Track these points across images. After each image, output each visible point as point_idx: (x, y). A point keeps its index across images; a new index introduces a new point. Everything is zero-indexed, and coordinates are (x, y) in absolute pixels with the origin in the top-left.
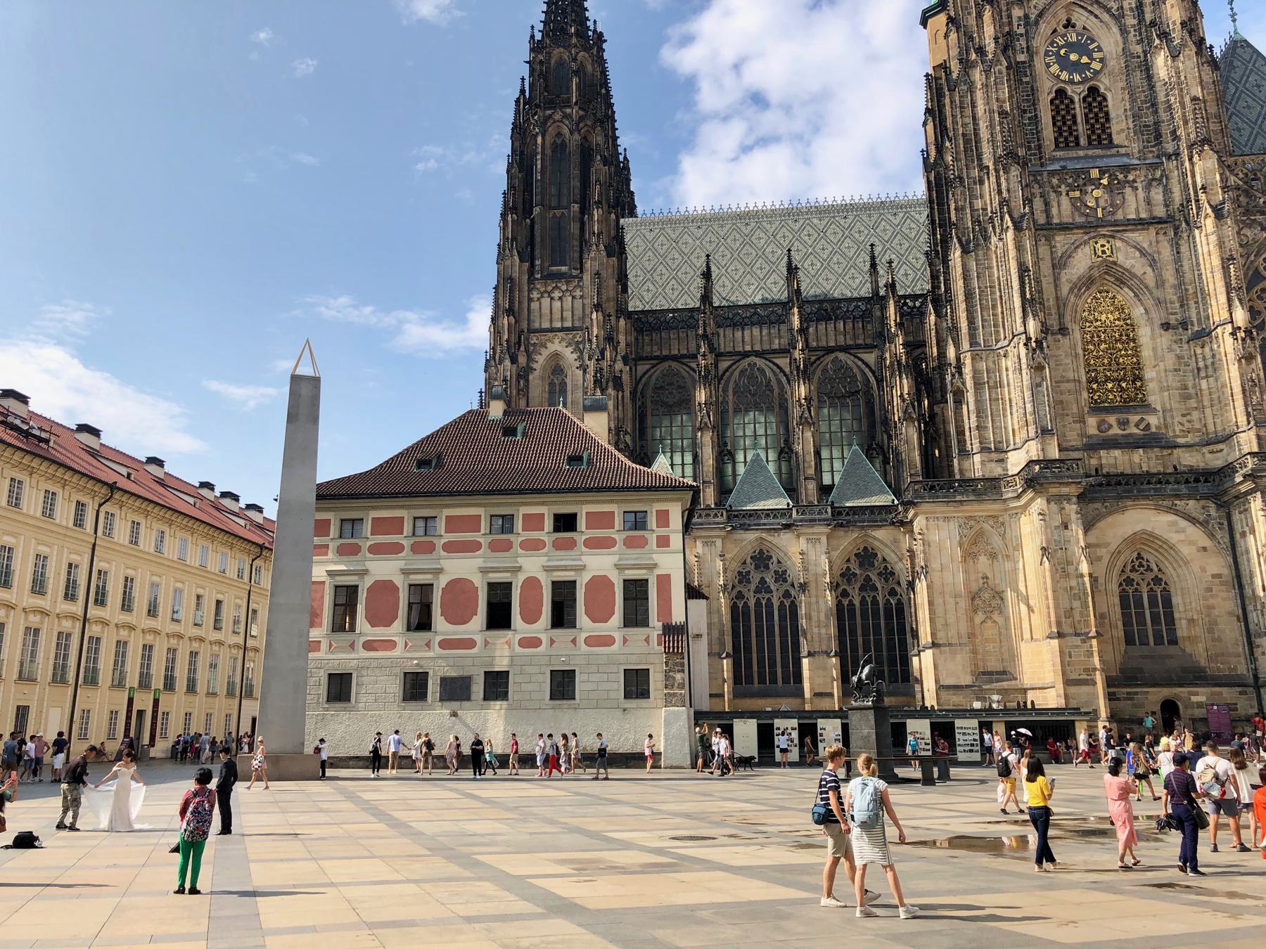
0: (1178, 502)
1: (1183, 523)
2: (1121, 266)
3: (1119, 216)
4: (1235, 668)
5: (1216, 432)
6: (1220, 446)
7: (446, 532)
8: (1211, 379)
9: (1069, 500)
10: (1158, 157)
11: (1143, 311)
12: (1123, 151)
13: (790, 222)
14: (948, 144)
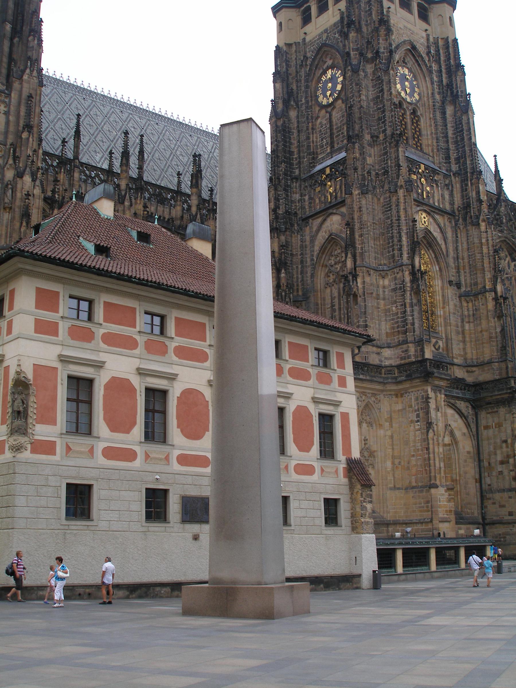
0: (457, 401)
1: (457, 416)
2: (433, 235)
3: (431, 201)
4: (473, 513)
5: (472, 359)
6: (474, 369)
7: (176, 335)
8: (472, 324)
9: (440, 391)
10: (447, 171)
11: (438, 269)
12: (431, 158)
13: (118, 111)
14: (292, 103)
